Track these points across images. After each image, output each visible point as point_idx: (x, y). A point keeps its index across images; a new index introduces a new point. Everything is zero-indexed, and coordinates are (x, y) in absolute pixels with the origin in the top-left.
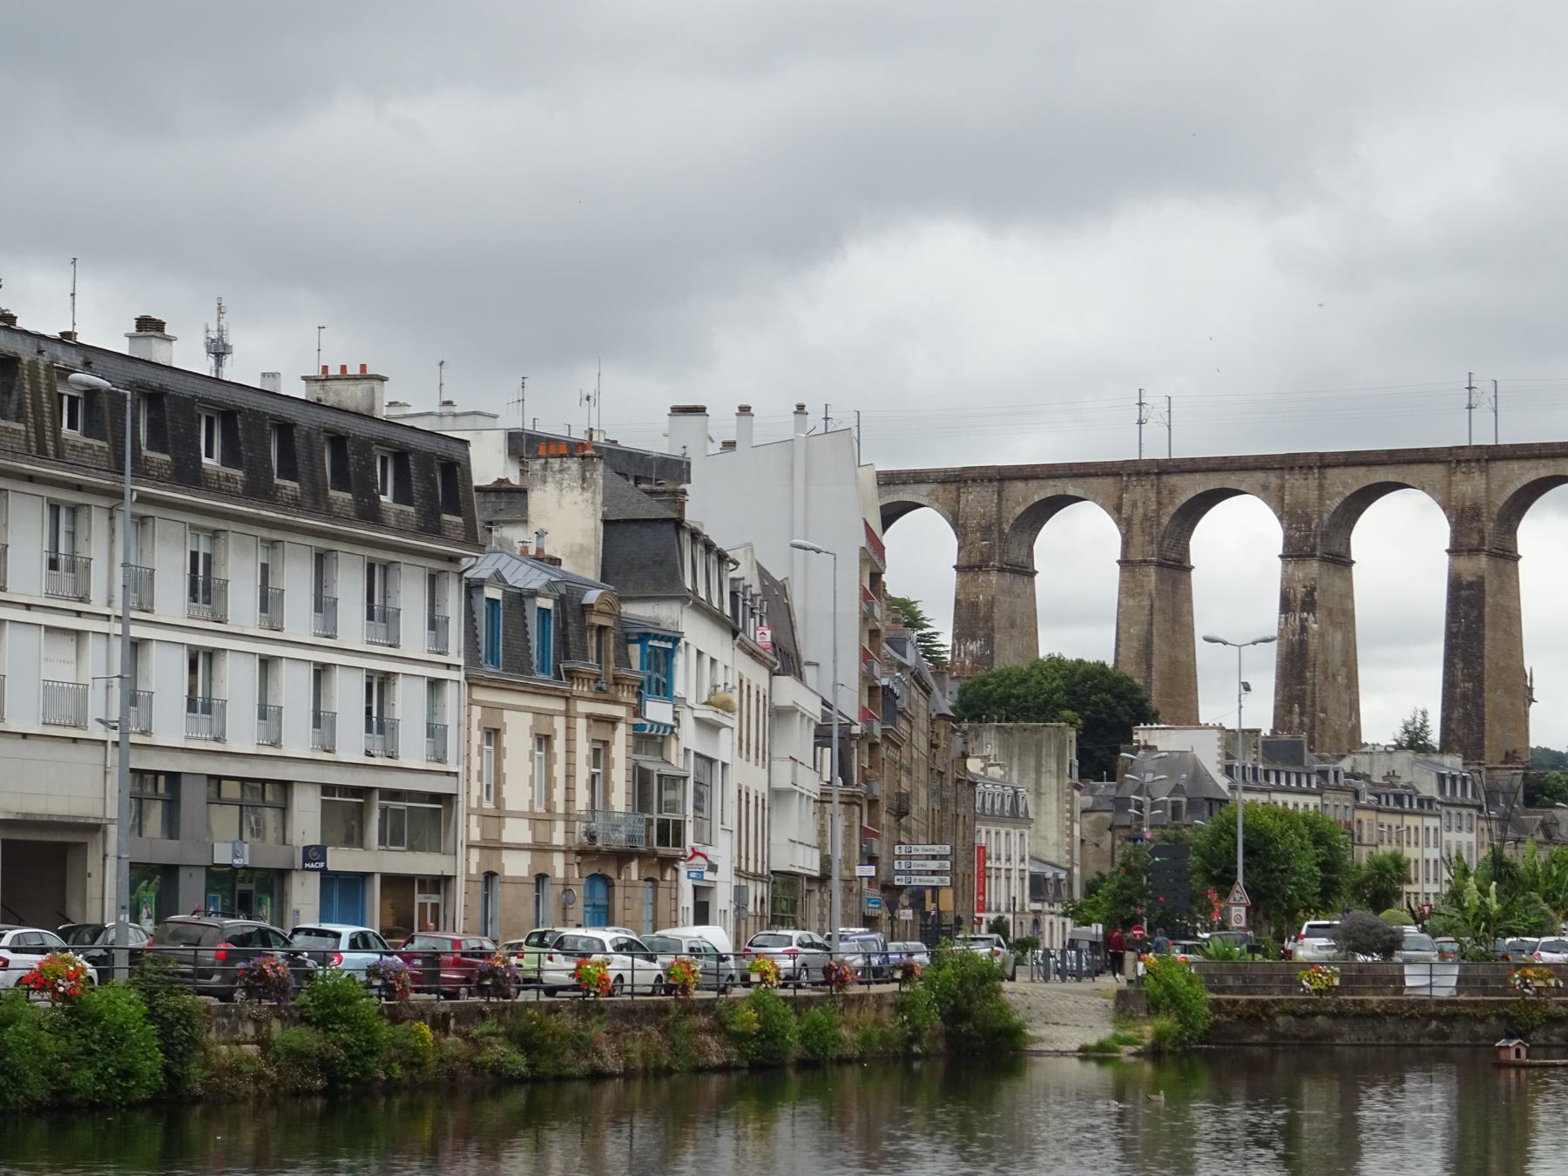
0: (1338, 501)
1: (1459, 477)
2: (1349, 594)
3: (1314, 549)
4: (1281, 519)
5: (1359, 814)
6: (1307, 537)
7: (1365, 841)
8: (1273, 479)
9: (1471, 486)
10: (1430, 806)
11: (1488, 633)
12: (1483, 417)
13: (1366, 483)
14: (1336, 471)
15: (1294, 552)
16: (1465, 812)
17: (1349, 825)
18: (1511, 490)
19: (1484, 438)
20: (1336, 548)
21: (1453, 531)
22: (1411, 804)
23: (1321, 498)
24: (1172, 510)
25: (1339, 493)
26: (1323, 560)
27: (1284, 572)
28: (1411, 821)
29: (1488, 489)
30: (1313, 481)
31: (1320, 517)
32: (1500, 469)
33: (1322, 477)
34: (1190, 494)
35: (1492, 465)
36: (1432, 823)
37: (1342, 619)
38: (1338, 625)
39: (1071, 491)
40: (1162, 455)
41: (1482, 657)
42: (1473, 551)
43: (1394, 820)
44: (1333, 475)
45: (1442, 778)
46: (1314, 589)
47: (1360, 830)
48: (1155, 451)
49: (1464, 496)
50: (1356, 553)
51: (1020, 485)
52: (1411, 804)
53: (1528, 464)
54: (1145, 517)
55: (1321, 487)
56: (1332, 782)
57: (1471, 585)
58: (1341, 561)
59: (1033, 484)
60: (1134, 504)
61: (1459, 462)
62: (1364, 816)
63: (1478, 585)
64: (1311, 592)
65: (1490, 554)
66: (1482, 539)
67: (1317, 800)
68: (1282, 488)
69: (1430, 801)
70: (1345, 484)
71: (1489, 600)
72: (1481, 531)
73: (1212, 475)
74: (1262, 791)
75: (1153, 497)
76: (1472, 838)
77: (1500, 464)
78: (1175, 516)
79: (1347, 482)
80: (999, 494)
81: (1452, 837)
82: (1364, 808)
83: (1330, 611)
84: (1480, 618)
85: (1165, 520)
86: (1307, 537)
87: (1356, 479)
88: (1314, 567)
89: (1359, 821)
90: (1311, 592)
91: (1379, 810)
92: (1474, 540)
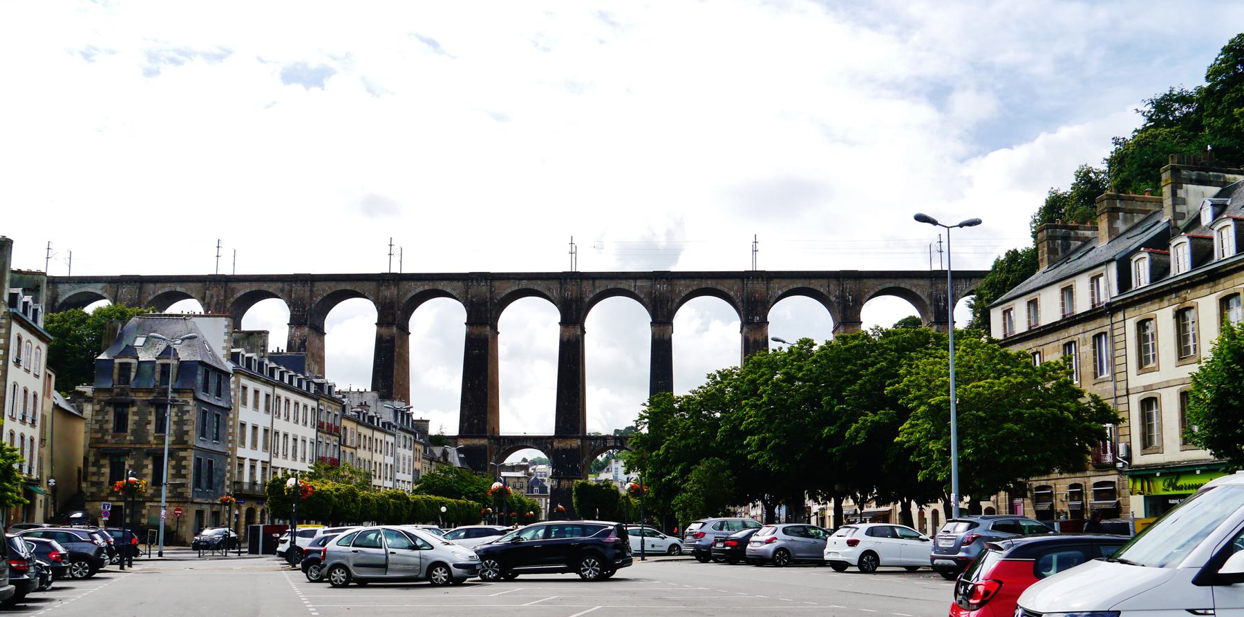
0: (320, 298)
2: (322, 348)
5: (345, 423)
8: (286, 287)
9: (390, 292)
11: (396, 366)
13: (334, 290)
15: (295, 322)
16: (408, 436)
17: (337, 429)
19: (395, 269)
24: (232, 300)
26: (311, 327)
30: (307, 288)
32: (405, 285)
33: (312, 286)
34: (242, 293)
36: (390, 439)
38: (317, 362)
39: (179, 289)
40: (229, 272)
42: (389, 325)
43: (368, 432)
44: (319, 286)
45: (396, 412)
48: (226, 270)
51: (152, 286)
54: (217, 303)
55: (311, 291)
57: (388, 341)
58: (321, 332)
59: (158, 285)
60: (212, 296)
62: (350, 425)
63: (392, 340)
64: (303, 343)
65: (398, 328)
67: (315, 404)
69: (390, 424)
72: (394, 315)
74: (267, 383)
75: (222, 293)
76: (411, 453)
78: (233, 304)
79: (325, 289)
80: (140, 289)
81: (401, 451)
82: (349, 418)
85: (228, 305)
90: (303, 343)
91: (358, 423)
92: (390, 318)
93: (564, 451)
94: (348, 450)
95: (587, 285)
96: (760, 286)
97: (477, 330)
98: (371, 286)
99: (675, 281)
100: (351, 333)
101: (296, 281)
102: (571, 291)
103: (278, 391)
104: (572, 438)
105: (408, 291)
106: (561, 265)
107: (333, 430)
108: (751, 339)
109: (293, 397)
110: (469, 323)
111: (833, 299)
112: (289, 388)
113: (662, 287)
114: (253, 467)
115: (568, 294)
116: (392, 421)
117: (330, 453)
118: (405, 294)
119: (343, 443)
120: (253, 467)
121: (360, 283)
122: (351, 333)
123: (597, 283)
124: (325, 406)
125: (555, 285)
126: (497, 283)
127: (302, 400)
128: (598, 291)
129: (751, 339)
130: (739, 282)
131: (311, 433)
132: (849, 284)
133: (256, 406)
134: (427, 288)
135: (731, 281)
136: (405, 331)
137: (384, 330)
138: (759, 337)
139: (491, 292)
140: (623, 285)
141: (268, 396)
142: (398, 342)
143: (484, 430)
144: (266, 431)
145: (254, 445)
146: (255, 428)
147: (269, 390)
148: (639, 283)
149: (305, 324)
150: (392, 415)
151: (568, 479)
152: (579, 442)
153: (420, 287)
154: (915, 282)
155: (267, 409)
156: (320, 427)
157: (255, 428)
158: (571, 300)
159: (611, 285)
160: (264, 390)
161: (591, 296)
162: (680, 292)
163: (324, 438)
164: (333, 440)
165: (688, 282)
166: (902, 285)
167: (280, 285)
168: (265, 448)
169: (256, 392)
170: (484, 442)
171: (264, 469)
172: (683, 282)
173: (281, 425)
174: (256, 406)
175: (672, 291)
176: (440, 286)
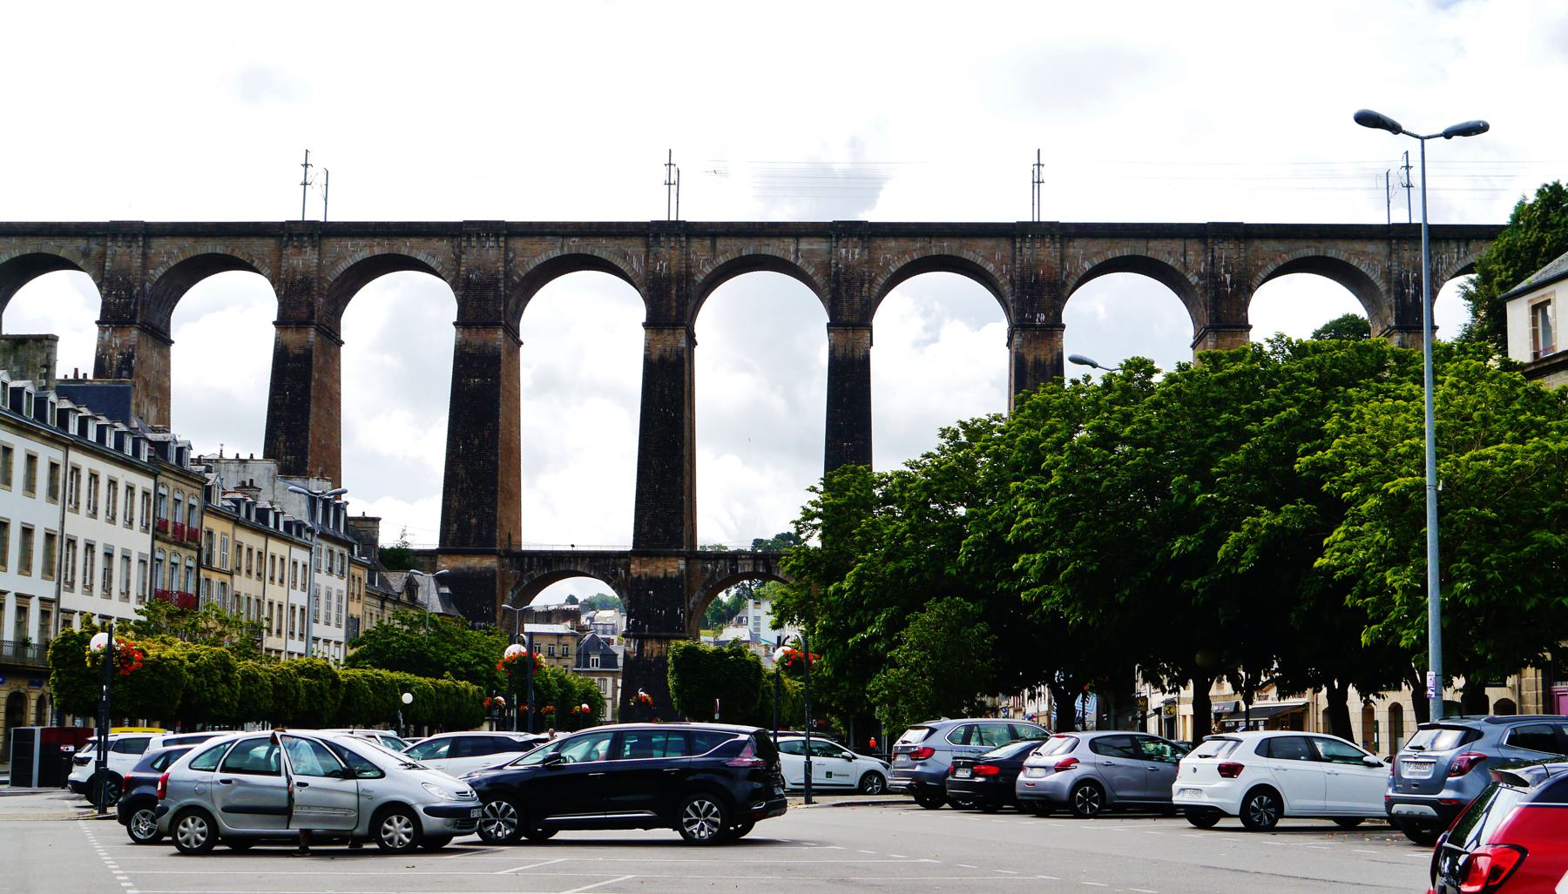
1: (290, 251)
2: (166, 372)
3: (134, 316)
4: (100, 286)
5: (210, 522)
6: (127, 304)
7: (216, 564)
8: (95, 247)
9: (303, 260)
10: (299, 534)
11: (313, 409)
12: (315, 194)
13: (192, 254)
14: (162, 241)
15: (110, 319)
16: (337, 549)
18: (343, 266)
19: (315, 214)
20: (156, 322)
21: (280, 304)
22: (277, 525)
23: (144, 267)
25: (162, 263)
27: (101, 338)
28: (277, 548)
29: (319, 264)
30: (137, 251)
31: (143, 286)
32: (333, 245)
33: (146, 246)
35: (325, 241)
36: (301, 556)
37: (157, 394)
38: (154, 400)
41: (306, 429)
42: (302, 325)
44: (158, 245)
45: (313, 500)
46: (131, 356)
47: (211, 547)
49: (294, 271)
50: (174, 335)
52: (277, 525)
53: (362, 242)
55: (144, 255)
56: (173, 461)
57: (298, 358)
58: (161, 338)
61: (291, 236)
63: (306, 357)
64: (127, 360)
65: (319, 331)
66: (312, 313)
67: (143, 483)
68: (103, 255)
69: (300, 525)
70: (170, 254)
71: (316, 375)
72: (311, 305)
73: (29, 240)
74: (52, 440)
77: (333, 241)
79: (169, 253)
81: (322, 580)
82: (218, 514)
83: (146, 384)
84: (308, 387)
86: (127, 304)
87: (182, 250)
88: (134, 334)
89: (210, 533)
90: (127, 360)
91: (237, 523)
92: (303, 312)
93: (653, 582)
94: (216, 578)
95: (699, 249)
96: (1047, 253)
97: (477, 338)
98: (266, 246)
99: (879, 242)
100: (223, 342)
101: (114, 236)
102: (668, 257)
103: (76, 457)
104: (666, 556)
105: (340, 257)
106: (648, 209)
107: (186, 537)
108: (1030, 358)
109: (106, 470)
110: (463, 322)
111: (1193, 279)
112: (97, 451)
113: (851, 253)
114: (22, 611)
115: (661, 266)
116: (305, 519)
117: (180, 584)
118: (334, 264)
119: (204, 562)
120: (22, 611)
121: (243, 242)
122: (223, 342)
123: (721, 243)
124: (170, 486)
125: (635, 247)
126: (518, 244)
127: (124, 476)
128: (722, 260)
129: (1030, 358)
130: (1005, 244)
131: (140, 542)
132: (1226, 251)
133: (30, 487)
134: (377, 251)
135: (990, 243)
136: (332, 338)
137: (291, 337)
138: (1044, 355)
139: (507, 262)
140: (773, 248)
141: (54, 467)
142: (317, 360)
143: (491, 540)
144: (50, 537)
145: (25, 566)
146: (27, 532)
147: (57, 454)
148: (804, 245)
149: (131, 322)
150: (304, 507)
151: (659, 639)
152: (682, 564)
153: (362, 251)
154: (1357, 246)
155: (53, 493)
156: (159, 531)
157: (27, 532)
158: (669, 279)
159: (749, 248)
160: (47, 454)
161: (708, 270)
162: (887, 263)
163: (168, 553)
164: (186, 558)
165: (903, 243)
166: (1332, 253)
167: (81, 243)
168: (48, 571)
169: (31, 459)
170: (489, 562)
171: (45, 614)
172: (892, 243)
173: (80, 526)
174: (30, 487)
175: (871, 261)
176: (405, 247)
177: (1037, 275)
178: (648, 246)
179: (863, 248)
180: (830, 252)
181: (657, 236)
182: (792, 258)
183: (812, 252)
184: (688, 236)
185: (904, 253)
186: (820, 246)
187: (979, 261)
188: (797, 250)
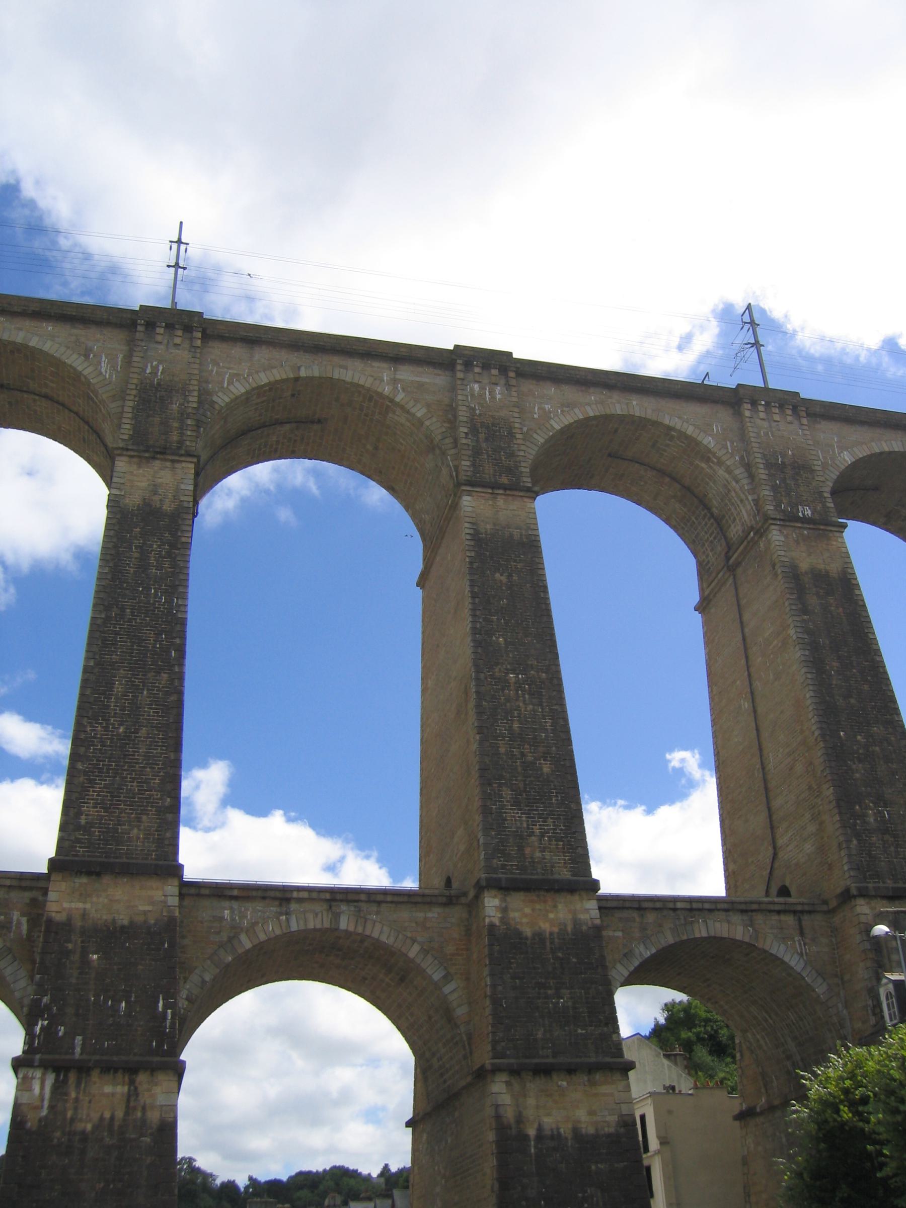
108: (804, 566)
123: (262, 355)
129: (804, 566)
148: (406, 373)
161: (239, 389)
172: (551, 390)
177: (784, 456)
178: (131, 343)
179: (508, 386)
180: (453, 389)
181: (150, 326)
182: (387, 390)
183: (421, 386)
184: (206, 337)
185: (571, 405)
186: (434, 379)
187: (690, 430)
188: (394, 381)
